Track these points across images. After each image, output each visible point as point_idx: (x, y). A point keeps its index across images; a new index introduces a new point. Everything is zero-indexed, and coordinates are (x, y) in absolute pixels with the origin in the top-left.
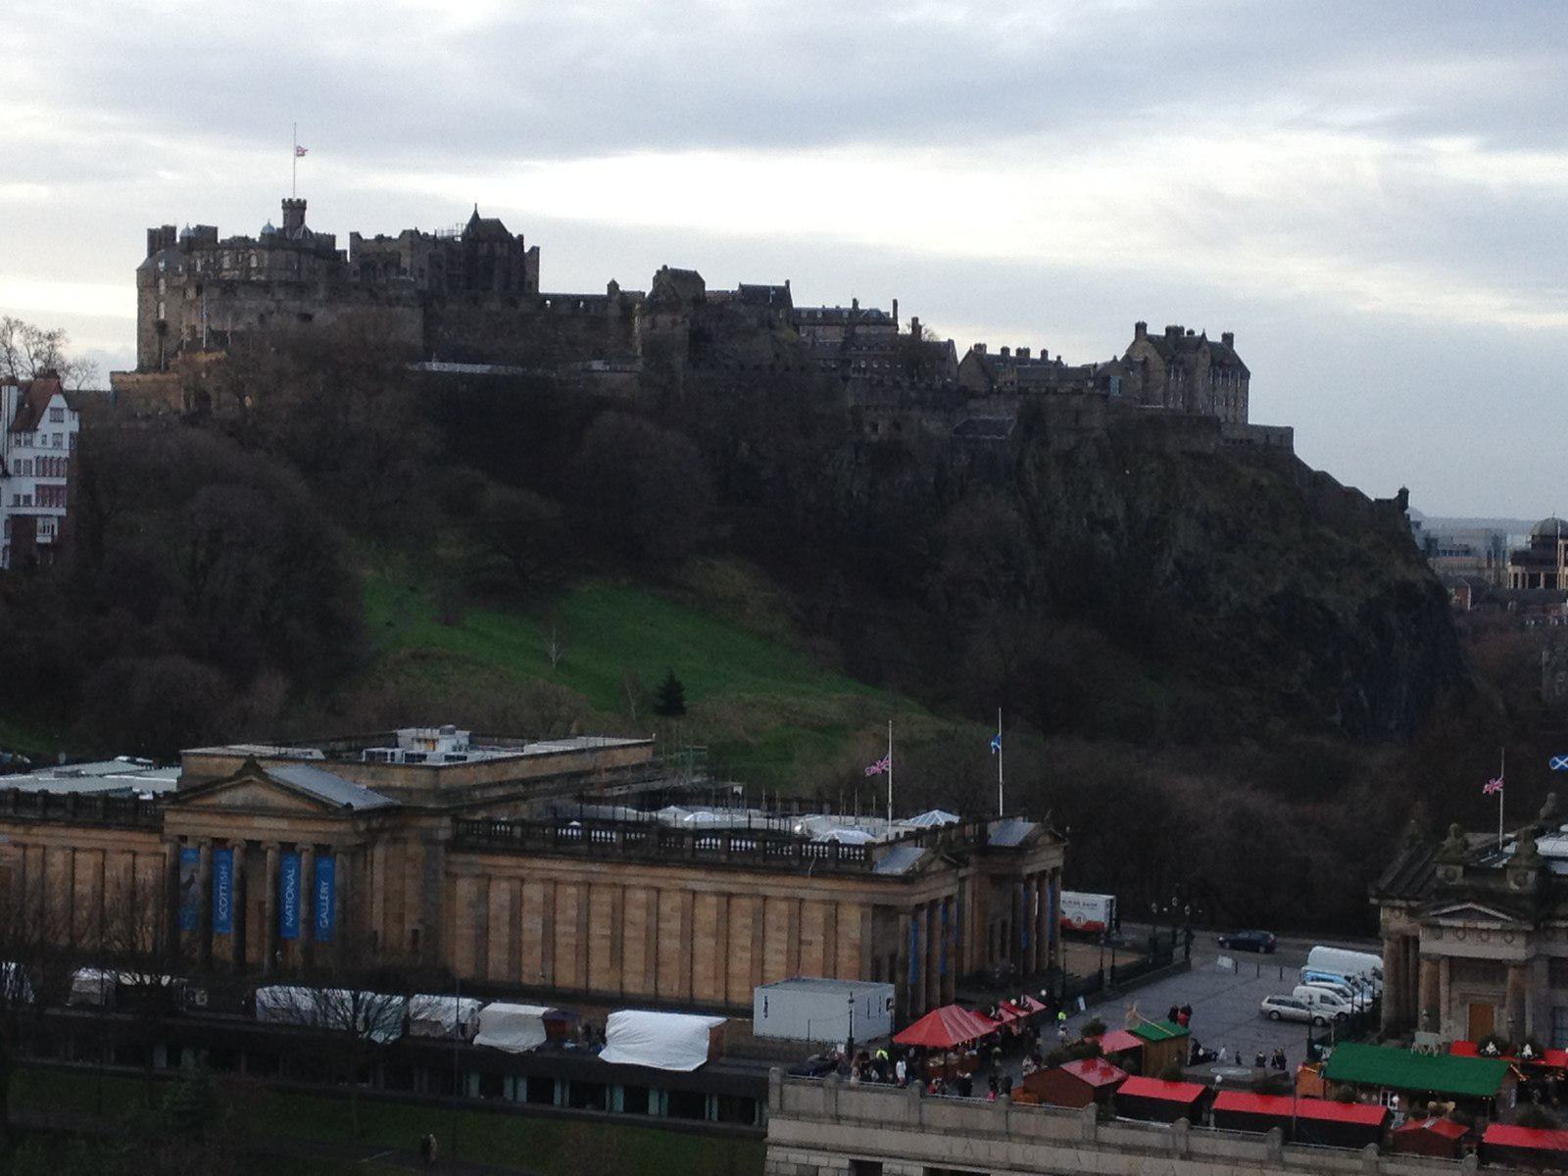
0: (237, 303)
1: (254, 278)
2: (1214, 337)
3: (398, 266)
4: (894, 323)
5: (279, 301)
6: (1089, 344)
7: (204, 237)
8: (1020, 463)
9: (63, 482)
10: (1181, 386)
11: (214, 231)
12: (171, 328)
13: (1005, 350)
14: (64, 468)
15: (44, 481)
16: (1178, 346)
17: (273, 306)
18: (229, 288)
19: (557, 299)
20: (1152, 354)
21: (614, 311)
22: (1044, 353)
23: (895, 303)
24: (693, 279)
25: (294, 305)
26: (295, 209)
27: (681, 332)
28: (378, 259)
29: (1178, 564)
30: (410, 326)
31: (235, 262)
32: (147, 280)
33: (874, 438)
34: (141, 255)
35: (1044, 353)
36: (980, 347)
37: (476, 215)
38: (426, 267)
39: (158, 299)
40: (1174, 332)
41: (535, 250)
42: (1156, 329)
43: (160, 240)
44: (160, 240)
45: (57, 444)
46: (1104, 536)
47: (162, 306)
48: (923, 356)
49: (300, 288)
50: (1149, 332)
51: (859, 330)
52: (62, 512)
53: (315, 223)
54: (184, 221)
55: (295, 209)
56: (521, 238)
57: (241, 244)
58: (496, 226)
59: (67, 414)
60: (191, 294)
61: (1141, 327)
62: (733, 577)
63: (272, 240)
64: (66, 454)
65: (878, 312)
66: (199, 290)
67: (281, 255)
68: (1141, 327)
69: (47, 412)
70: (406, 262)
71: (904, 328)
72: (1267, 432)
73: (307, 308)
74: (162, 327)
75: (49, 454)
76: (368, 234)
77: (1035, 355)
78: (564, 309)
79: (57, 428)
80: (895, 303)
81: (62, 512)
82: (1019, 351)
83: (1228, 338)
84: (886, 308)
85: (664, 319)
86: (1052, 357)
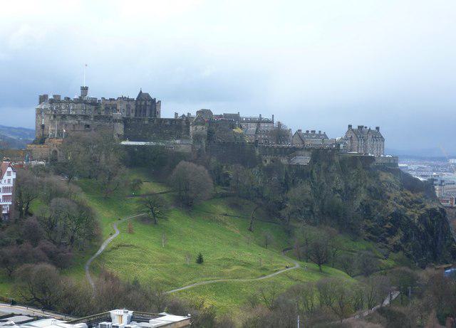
1: (71, 113)
2: (373, 128)
4: (272, 122)
5: (79, 121)
6: (336, 132)
7: (56, 100)
8: (312, 172)
9: (11, 194)
13: (308, 131)
15: (5, 194)
17: (77, 122)
18: (64, 117)
19: (166, 120)
20: (353, 135)
22: (320, 132)
24: (209, 112)
25: (84, 122)
26: (85, 89)
27: (205, 132)
28: (111, 105)
29: (361, 203)
30: (120, 129)
35: (320, 132)
37: (141, 92)
39: (42, 118)
40: (361, 127)
42: (355, 127)
43: (43, 99)
46: (338, 195)
48: (280, 133)
49: (85, 117)
51: (262, 125)
52: (11, 203)
53: (91, 95)
56: (155, 99)
59: (12, 173)
60: (52, 118)
61: (350, 126)
62: (220, 208)
63: (80, 101)
64: (12, 185)
66: (55, 117)
67: (80, 105)
68: (350, 126)
69: (6, 173)
70: (119, 107)
71: (275, 125)
73: (88, 123)
74: (43, 127)
75: (7, 186)
77: (317, 132)
79: (9, 177)
82: (312, 131)
83: (377, 128)
84: (270, 118)
85: (199, 127)
86: (322, 133)
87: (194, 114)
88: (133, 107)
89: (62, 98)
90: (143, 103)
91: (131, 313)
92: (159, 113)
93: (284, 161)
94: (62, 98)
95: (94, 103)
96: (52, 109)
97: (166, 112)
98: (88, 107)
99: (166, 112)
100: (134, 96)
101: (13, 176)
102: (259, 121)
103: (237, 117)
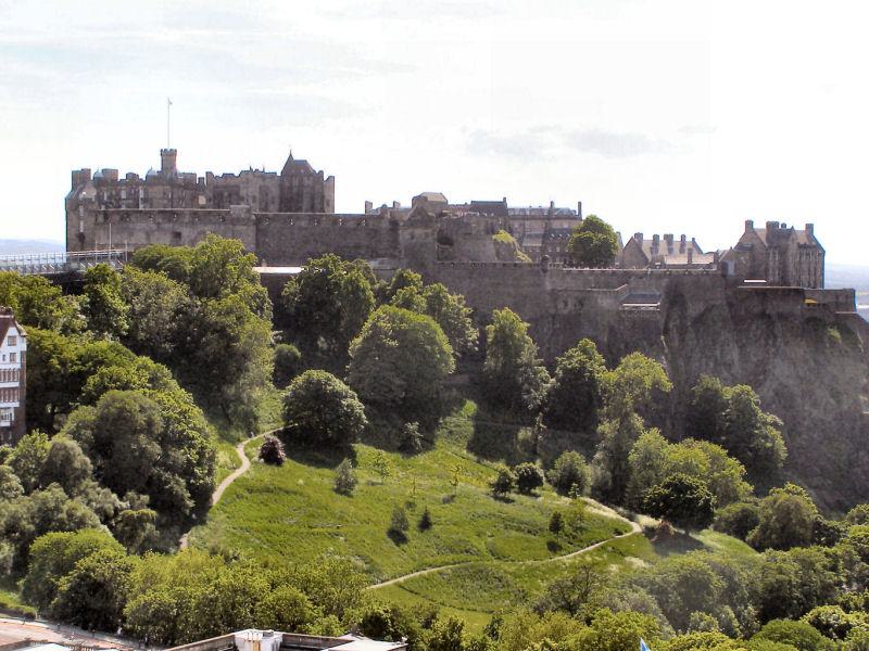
0: (131, 226)
1: (141, 208)
3: (238, 194)
4: (578, 217)
7: (106, 180)
9: (17, 384)
10: (777, 263)
11: (115, 172)
12: (87, 239)
13: (656, 237)
14: (17, 376)
16: (778, 234)
17: (154, 227)
19: (347, 218)
21: (385, 225)
22: (683, 237)
23: (580, 204)
25: (167, 226)
26: (168, 156)
28: (224, 191)
31: (129, 194)
32: (73, 205)
33: (565, 312)
34: (66, 187)
35: (683, 237)
36: (639, 236)
38: (257, 195)
39: (79, 218)
41: (332, 179)
42: (760, 225)
43: (80, 178)
44: (80, 178)
45: (12, 360)
47: (82, 223)
50: (755, 226)
52: (17, 404)
53: (183, 166)
54: (95, 167)
55: (168, 156)
56: (321, 172)
57: (132, 177)
58: (303, 164)
59: (18, 340)
60: (101, 219)
61: (749, 224)
63: (152, 180)
64: (18, 366)
65: (569, 211)
68: (749, 224)
69: (6, 339)
70: (243, 192)
72: (837, 293)
75: (8, 367)
76: (218, 172)
77: (677, 238)
78: (351, 225)
79: (13, 349)
80: (580, 204)
81: (17, 404)
83: (810, 227)
84: (574, 207)
85: (419, 232)
87: (406, 203)
88: (275, 192)
89: (122, 176)
90: (296, 182)
91: (278, 636)
92: (330, 203)
93: (605, 302)
94: (122, 176)
95: (190, 185)
96: (99, 197)
97: (347, 202)
98: (179, 193)
99: (347, 202)
100: (276, 166)
101: (22, 346)
102: (550, 215)
103: (499, 208)
